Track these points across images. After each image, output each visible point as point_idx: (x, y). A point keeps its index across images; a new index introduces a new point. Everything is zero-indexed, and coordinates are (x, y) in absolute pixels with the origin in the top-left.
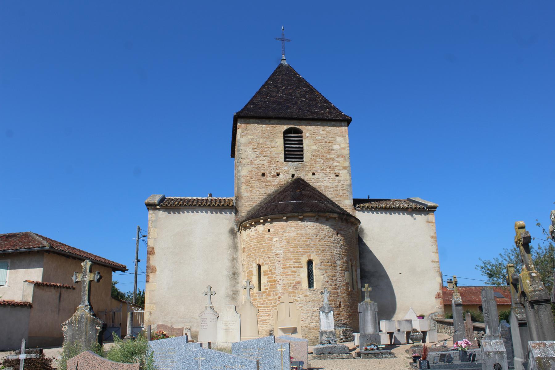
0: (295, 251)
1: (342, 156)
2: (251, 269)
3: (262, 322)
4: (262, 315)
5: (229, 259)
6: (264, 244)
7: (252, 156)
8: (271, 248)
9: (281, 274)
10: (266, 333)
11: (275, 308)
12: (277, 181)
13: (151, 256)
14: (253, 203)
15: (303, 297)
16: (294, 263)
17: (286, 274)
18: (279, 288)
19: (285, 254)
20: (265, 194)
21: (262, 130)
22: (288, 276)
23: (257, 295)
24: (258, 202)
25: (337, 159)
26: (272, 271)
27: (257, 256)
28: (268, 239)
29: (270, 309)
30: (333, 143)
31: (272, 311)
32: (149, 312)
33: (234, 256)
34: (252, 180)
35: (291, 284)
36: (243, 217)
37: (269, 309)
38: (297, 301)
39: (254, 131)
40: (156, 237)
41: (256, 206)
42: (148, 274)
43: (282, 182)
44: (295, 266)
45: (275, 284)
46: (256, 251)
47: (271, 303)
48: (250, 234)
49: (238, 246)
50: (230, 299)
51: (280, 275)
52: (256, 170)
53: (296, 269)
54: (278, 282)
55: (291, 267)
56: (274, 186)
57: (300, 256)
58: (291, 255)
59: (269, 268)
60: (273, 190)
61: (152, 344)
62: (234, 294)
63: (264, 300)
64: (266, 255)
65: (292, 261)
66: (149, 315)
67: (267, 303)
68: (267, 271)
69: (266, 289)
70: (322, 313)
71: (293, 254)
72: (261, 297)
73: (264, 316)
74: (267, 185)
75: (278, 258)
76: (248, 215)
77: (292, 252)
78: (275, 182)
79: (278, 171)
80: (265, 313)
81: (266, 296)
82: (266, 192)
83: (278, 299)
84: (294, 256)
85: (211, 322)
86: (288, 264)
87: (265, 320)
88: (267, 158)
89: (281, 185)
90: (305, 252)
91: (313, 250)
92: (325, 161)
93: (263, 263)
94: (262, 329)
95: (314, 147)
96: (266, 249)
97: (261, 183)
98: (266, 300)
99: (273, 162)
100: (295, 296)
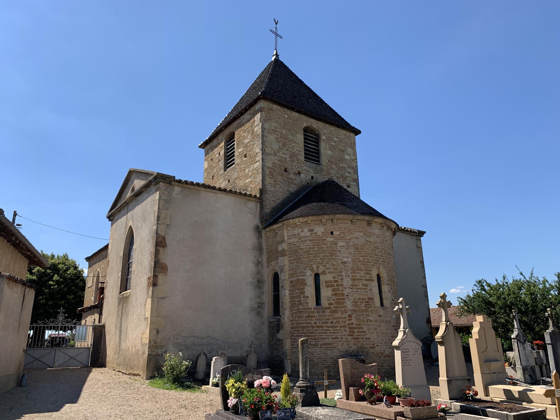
0: (366, 261)
1: (352, 168)
3: (324, 346)
4: (324, 337)
5: (253, 262)
6: (325, 249)
7: (276, 146)
8: (336, 254)
9: (350, 286)
10: (332, 361)
11: (345, 328)
12: (298, 180)
13: (161, 250)
14: (277, 199)
15: (377, 317)
16: (364, 275)
18: (349, 304)
19: (354, 263)
20: (289, 193)
22: (359, 290)
23: (316, 311)
24: (281, 199)
25: (348, 170)
26: (338, 282)
27: (314, 262)
28: (332, 242)
32: (156, 329)
33: (259, 259)
34: (276, 174)
35: (363, 299)
36: (267, 214)
37: (336, 330)
38: (371, 322)
40: (168, 223)
41: (280, 203)
42: (157, 274)
44: (366, 278)
45: (343, 299)
46: (312, 256)
47: (339, 322)
48: (299, 234)
49: (263, 248)
51: (349, 288)
52: (279, 163)
55: (362, 280)
56: (296, 185)
57: (371, 267)
58: (362, 264)
59: (334, 278)
60: (295, 189)
61: (324, 392)
62: (259, 307)
63: (327, 317)
65: (363, 272)
66: (156, 334)
67: (332, 323)
68: (331, 281)
72: (323, 314)
73: (328, 339)
74: (290, 183)
75: (345, 266)
76: (272, 212)
77: (363, 262)
78: (297, 181)
79: (299, 169)
80: (329, 334)
81: (331, 313)
83: (347, 318)
84: (365, 267)
85: (414, 354)
86: (358, 275)
87: (331, 344)
88: (289, 152)
90: (375, 263)
91: (381, 262)
94: (325, 355)
95: (330, 152)
96: (329, 255)
97: (284, 178)
98: (331, 318)
99: (295, 159)
100: (368, 316)
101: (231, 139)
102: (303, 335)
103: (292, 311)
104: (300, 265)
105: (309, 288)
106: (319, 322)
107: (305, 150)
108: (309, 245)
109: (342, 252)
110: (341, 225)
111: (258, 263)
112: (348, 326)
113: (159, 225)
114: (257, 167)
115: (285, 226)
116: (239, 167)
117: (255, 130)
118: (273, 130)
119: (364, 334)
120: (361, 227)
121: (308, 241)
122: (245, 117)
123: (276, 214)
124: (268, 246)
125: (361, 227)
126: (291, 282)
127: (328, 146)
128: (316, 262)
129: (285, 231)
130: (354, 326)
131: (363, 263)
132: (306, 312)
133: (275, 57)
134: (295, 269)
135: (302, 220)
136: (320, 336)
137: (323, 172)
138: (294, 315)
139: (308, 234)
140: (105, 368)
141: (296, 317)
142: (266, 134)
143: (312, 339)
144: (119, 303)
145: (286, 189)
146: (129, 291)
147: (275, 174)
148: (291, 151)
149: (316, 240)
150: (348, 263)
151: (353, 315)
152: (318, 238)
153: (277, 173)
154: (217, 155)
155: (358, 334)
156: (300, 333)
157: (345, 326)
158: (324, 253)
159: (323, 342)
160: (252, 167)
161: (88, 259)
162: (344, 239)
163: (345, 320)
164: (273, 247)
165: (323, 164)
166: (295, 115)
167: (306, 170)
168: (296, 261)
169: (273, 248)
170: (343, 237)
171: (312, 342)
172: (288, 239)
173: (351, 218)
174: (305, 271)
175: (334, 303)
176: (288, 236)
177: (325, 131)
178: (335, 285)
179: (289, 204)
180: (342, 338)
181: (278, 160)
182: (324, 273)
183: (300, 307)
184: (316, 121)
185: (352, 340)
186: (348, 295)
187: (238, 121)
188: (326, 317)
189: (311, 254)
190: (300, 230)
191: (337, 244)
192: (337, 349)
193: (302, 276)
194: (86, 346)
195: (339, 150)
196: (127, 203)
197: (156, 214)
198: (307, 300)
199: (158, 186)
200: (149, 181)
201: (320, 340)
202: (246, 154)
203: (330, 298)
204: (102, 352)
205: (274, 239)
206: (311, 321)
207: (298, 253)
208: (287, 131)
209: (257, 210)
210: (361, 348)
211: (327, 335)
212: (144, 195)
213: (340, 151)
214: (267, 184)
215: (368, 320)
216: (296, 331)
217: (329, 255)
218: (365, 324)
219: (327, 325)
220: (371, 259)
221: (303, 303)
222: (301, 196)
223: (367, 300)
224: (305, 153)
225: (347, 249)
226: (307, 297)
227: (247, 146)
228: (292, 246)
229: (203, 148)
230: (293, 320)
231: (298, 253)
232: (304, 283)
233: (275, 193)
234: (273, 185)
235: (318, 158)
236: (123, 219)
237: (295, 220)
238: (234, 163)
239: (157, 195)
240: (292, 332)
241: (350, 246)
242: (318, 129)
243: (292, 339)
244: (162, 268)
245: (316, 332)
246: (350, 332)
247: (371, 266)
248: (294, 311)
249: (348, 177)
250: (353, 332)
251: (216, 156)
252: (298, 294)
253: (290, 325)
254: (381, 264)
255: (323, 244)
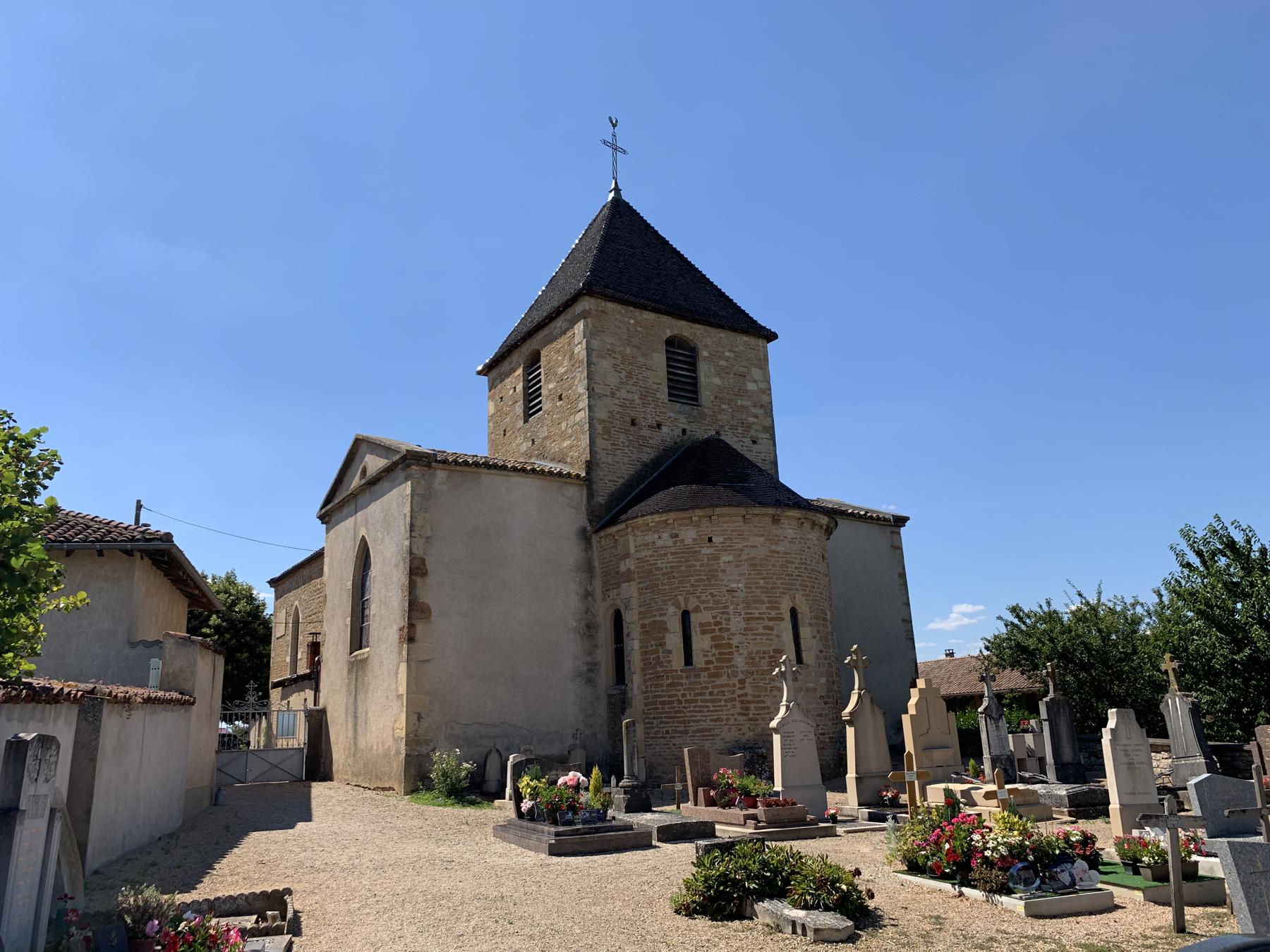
0: (770, 586)
1: (762, 406)
2: (658, 619)
6: (698, 568)
7: (613, 380)
8: (718, 576)
9: (743, 632)
11: (733, 703)
13: (418, 579)
14: (619, 478)
16: (768, 611)
17: (753, 632)
18: (740, 662)
19: (749, 591)
20: (639, 463)
21: (628, 330)
22: (758, 637)
23: (684, 675)
24: (626, 478)
25: (754, 410)
29: (721, 706)
30: (747, 378)
31: (726, 710)
32: (416, 713)
34: (615, 431)
35: (764, 653)
36: (601, 505)
37: (718, 706)
39: (614, 327)
40: (429, 534)
42: (413, 622)
43: (666, 441)
44: (770, 616)
47: (723, 692)
48: (654, 542)
49: (594, 567)
50: (583, 681)
51: (740, 634)
53: (772, 622)
54: (736, 649)
55: (763, 619)
56: (653, 447)
59: (714, 617)
60: (652, 456)
62: (591, 670)
63: (703, 685)
64: (706, 589)
65: (764, 607)
66: (417, 722)
67: (711, 694)
68: (709, 624)
69: (708, 662)
70: (990, 719)
71: (765, 593)
73: (705, 721)
75: (734, 597)
77: (762, 587)
79: (658, 418)
80: (708, 714)
82: (640, 459)
83: (738, 686)
86: (756, 612)
88: (638, 388)
89: (665, 446)
92: (735, 411)
93: (698, 607)
95: (717, 381)
96: (705, 578)
98: (710, 686)
99: (650, 399)
101: (533, 362)
102: (663, 715)
103: (645, 675)
104: (656, 596)
105: (672, 636)
106: (690, 694)
107: (669, 379)
108: (673, 562)
109: (728, 573)
110: (725, 525)
111: (587, 595)
112: (738, 699)
113: (413, 540)
114: (581, 421)
115: (630, 529)
116: (549, 418)
117: (576, 352)
118: (608, 350)
119: (767, 711)
120: (761, 527)
121: (669, 554)
122: (558, 325)
123: (618, 505)
124: (603, 563)
125: (761, 527)
126: (643, 626)
127: (712, 370)
128: (683, 591)
129: (631, 538)
130: (749, 698)
131: (765, 590)
132: (667, 677)
133: (612, 194)
134: (648, 604)
135: (659, 519)
136: (691, 716)
137: (705, 419)
138: (649, 684)
139: (670, 542)
140: (331, 782)
141: (651, 686)
142: (594, 359)
143: (678, 722)
144: (350, 671)
145: (634, 457)
146: (368, 649)
147: (613, 432)
148: (643, 386)
149: (682, 553)
150: (739, 591)
151: (748, 681)
152: (686, 548)
153: (617, 429)
154: (511, 392)
155: (755, 712)
156: (660, 713)
157: (733, 700)
158: (696, 575)
159: (697, 727)
160: (572, 420)
161: (273, 583)
162: (731, 550)
163: (733, 689)
164: (611, 565)
165: (703, 403)
166: (649, 316)
167: (672, 419)
168: (649, 591)
169: (612, 567)
170: (731, 546)
171: (679, 727)
172: (636, 551)
173: (742, 512)
174: (665, 607)
175: (715, 661)
176: (636, 547)
177: (708, 341)
178: (717, 630)
179: (641, 484)
180: (728, 719)
181: (619, 406)
182: (697, 609)
183: (659, 669)
184: (690, 324)
185: (745, 722)
186: (738, 647)
187: (546, 331)
188: (701, 684)
189: (674, 578)
190: (656, 536)
191: (719, 559)
192: (720, 737)
193: (661, 615)
194: (296, 746)
195: (735, 374)
196: (354, 496)
197: (408, 519)
198: (669, 657)
199: (409, 471)
200: (394, 463)
201: (692, 724)
202: (561, 395)
203: (708, 652)
204: (324, 755)
205: (612, 550)
206: (676, 693)
207: (653, 575)
208: (634, 350)
209: (582, 499)
210: (761, 735)
211: (703, 714)
212: (385, 484)
213: (737, 376)
214: (598, 450)
215: (773, 687)
216: (654, 709)
217: (705, 578)
218: (767, 695)
219: (703, 697)
220: (779, 582)
221: (662, 662)
222: (662, 469)
223: (772, 654)
224: (669, 387)
225: (737, 566)
226: (670, 652)
227: (562, 380)
228: (642, 564)
229: (485, 375)
230: (646, 692)
231: (653, 575)
232: (663, 628)
233: (614, 467)
234: (609, 452)
235: (696, 392)
236: (349, 523)
237: (646, 518)
238: (540, 409)
239: (407, 488)
240: (646, 711)
241: (741, 561)
242: (694, 338)
243: (646, 723)
244: (422, 611)
245: (685, 710)
246: (742, 708)
247: (778, 595)
248: (648, 677)
249: (754, 423)
250: (748, 709)
251: (508, 392)
252: (654, 647)
253: (642, 700)
254: (798, 590)
255: (695, 561)
